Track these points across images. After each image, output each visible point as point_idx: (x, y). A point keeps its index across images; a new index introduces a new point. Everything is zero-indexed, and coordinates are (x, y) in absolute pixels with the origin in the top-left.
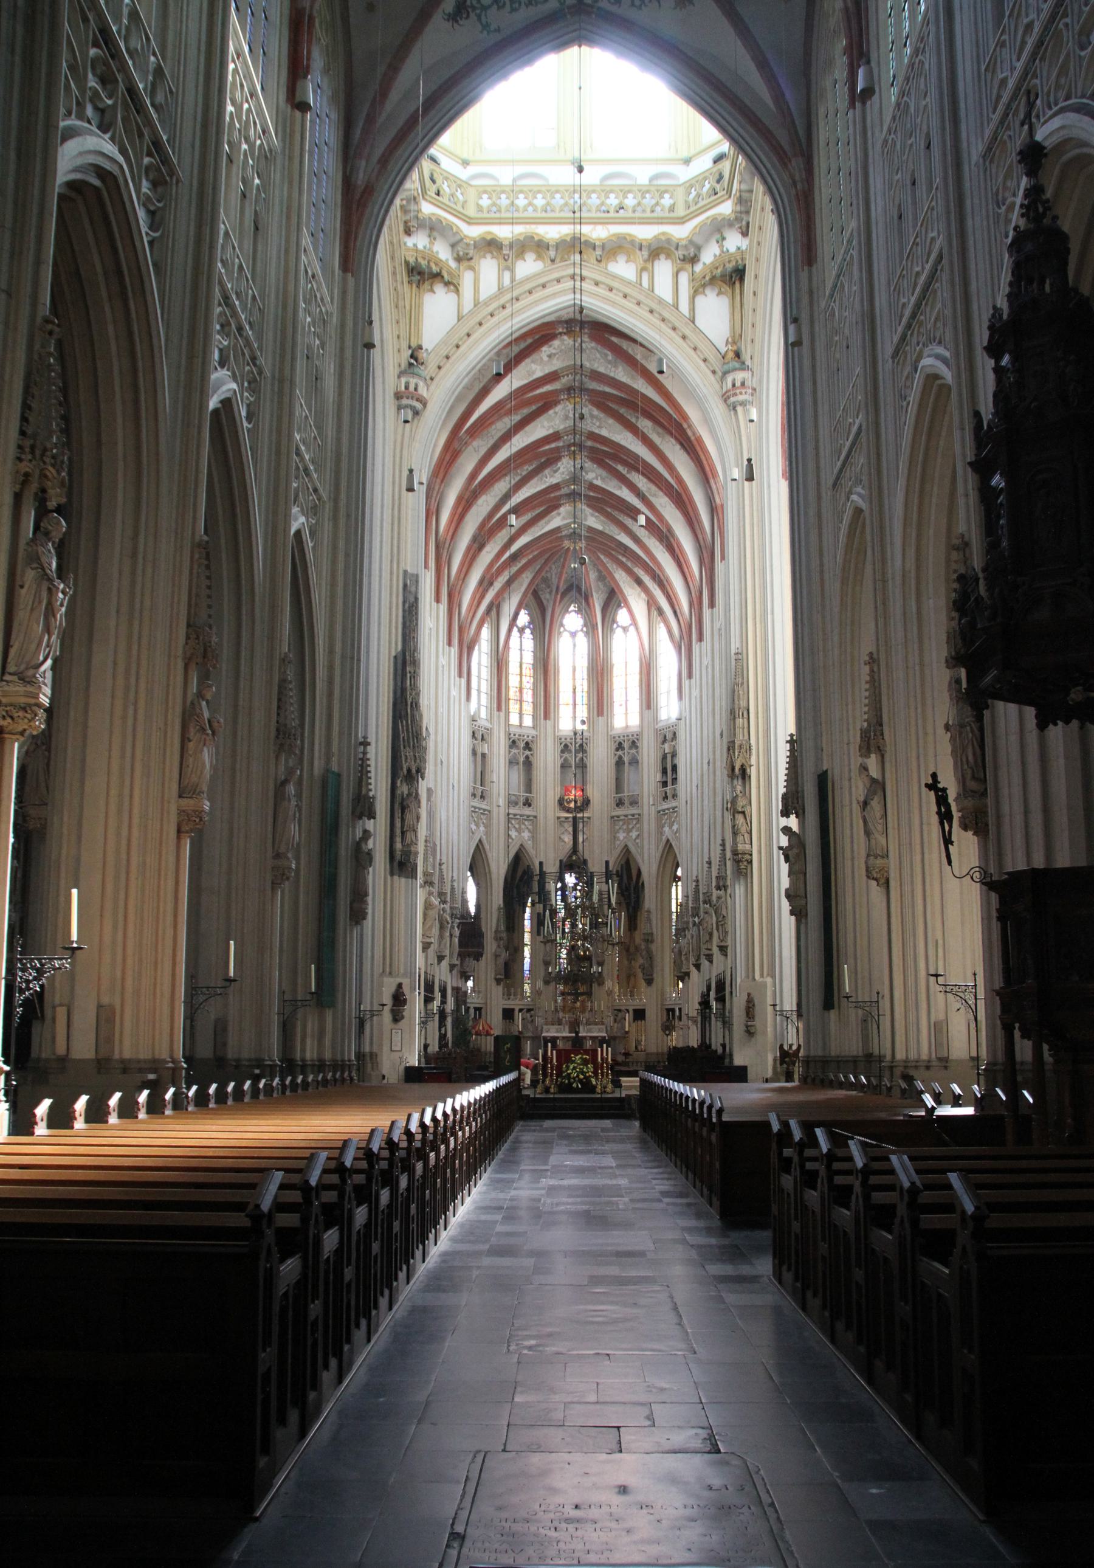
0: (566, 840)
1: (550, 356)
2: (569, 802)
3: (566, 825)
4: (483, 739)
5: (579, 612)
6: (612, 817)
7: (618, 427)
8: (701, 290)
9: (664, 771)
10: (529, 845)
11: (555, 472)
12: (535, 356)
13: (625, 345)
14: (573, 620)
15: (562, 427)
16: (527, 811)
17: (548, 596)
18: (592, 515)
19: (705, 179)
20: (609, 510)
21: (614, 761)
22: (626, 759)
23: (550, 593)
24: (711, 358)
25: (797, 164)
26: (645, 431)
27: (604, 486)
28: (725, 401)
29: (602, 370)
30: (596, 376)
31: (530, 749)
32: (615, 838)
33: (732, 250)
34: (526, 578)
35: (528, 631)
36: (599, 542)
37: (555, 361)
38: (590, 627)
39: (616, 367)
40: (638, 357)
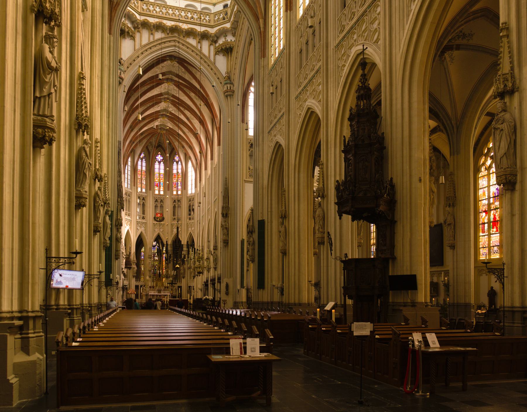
1: (162, 67)
4: (129, 196)
7: (183, 94)
8: (218, 53)
9: (190, 210)
11: (159, 106)
12: (158, 66)
13: (189, 67)
14: (159, 158)
15: (163, 92)
17: (151, 148)
18: (169, 123)
19: (221, 13)
20: (175, 122)
21: (173, 206)
22: (177, 206)
23: (152, 147)
24: (220, 78)
25: (261, 21)
26: (192, 97)
28: (224, 93)
29: (180, 74)
30: (178, 76)
33: (229, 40)
34: (145, 141)
35: (144, 160)
36: (171, 131)
37: (164, 69)
38: (165, 161)
39: (185, 74)
40: (193, 72)
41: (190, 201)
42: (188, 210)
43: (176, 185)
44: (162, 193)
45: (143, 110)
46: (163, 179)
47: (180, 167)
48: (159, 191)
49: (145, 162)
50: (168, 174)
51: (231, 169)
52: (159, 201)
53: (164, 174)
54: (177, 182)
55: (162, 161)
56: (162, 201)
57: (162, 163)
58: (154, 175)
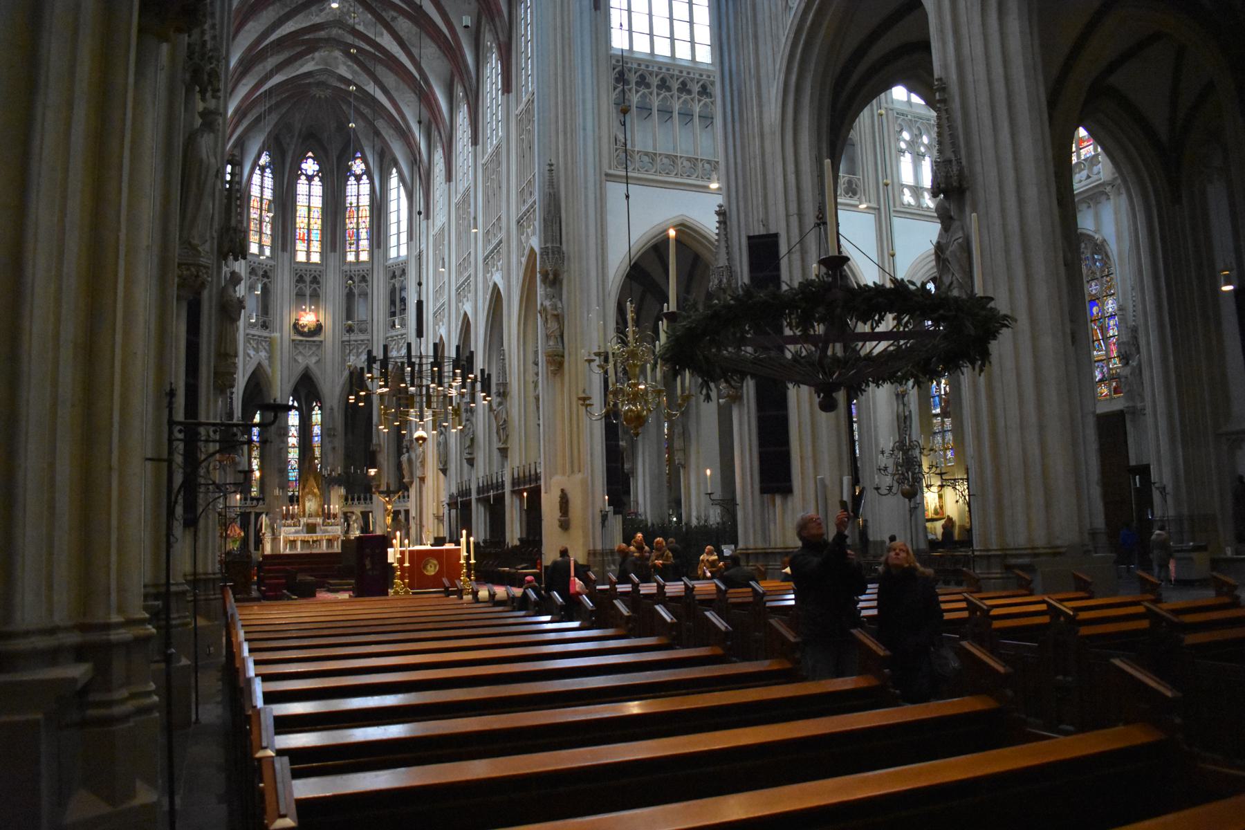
0: (300, 361)
2: (304, 326)
3: (300, 348)
5: (314, 159)
6: (343, 342)
9: (393, 303)
10: (265, 363)
11: (321, 11)
14: (310, 166)
16: (265, 333)
18: (344, 64)
22: (356, 291)
27: (365, 32)
31: (268, 277)
32: (344, 361)
34: (273, 119)
35: (268, 170)
41: (394, 276)
42: (388, 302)
43: (354, 238)
44: (315, 258)
45: (277, 17)
46: (319, 222)
47: (365, 188)
48: (308, 253)
49: (270, 176)
50: (334, 208)
51: (565, 139)
52: (308, 279)
53: (323, 208)
54: (358, 229)
55: (317, 175)
56: (315, 280)
57: (317, 179)
58: (296, 211)
